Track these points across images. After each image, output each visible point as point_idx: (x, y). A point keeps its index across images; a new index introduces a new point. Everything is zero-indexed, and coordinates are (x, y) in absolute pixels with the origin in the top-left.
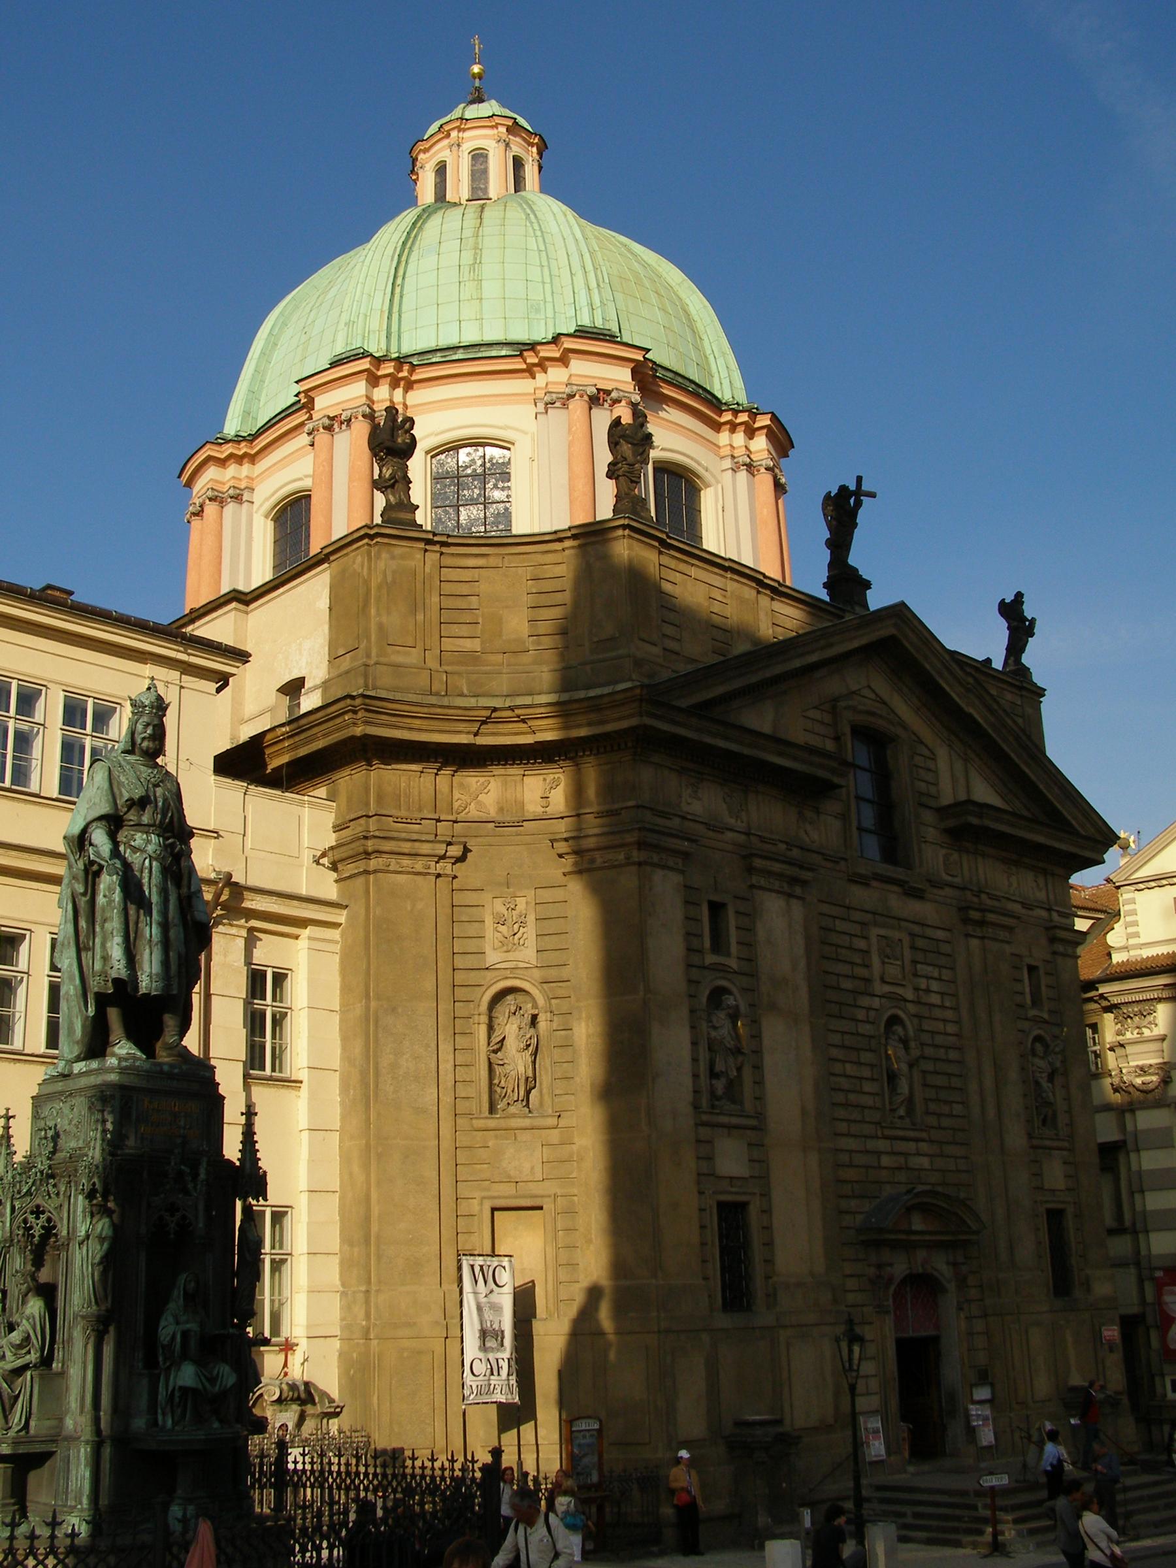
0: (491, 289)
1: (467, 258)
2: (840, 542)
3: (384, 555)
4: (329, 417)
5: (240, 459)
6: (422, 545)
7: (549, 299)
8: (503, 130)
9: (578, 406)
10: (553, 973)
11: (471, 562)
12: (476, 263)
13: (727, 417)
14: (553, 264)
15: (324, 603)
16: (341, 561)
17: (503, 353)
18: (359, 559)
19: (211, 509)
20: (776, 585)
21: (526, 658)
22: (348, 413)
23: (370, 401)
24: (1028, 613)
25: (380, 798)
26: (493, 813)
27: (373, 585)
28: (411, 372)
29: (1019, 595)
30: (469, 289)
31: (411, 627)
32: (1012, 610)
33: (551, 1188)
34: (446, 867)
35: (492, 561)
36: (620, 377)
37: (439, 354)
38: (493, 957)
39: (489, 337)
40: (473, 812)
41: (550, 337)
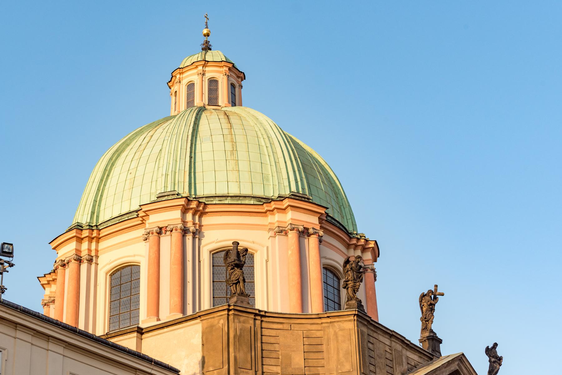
0: (243, 166)
1: (229, 146)
3: (236, 321)
4: (159, 227)
6: (252, 316)
7: (275, 174)
8: (227, 69)
9: (292, 236)
11: (275, 326)
12: (234, 150)
13: (354, 241)
14: (275, 154)
15: (197, 340)
16: (210, 320)
17: (252, 202)
18: (222, 321)
20: (408, 343)
22: (172, 227)
23: (184, 222)
28: (204, 208)
29: (496, 345)
30: (231, 165)
31: (249, 359)
35: (286, 326)
36: (312, 221)
37: (217, 199)
39: (245, 192)
41: (277, 195)
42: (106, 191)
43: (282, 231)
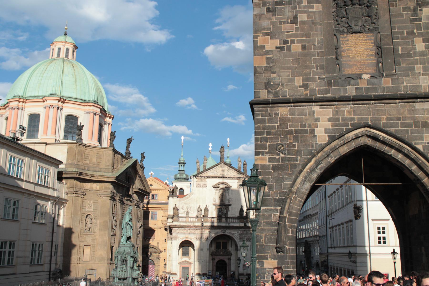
2: (128, 146)
5: (23, 102)
9: (92, 115)
10: (95, 213)
12: (76, 82)
19: (16, 110)
21: (95, 166)
24: (145, 155)
25: (76, 186)
26: (89, 188)
27: (77, 151)
29: (144, 153)
32: (142, 155)
33: (91, 243)
34: (82, 196)
38: (87, 210)
40: (86, 188)
42: (29, 85)
43: (89, 113)
